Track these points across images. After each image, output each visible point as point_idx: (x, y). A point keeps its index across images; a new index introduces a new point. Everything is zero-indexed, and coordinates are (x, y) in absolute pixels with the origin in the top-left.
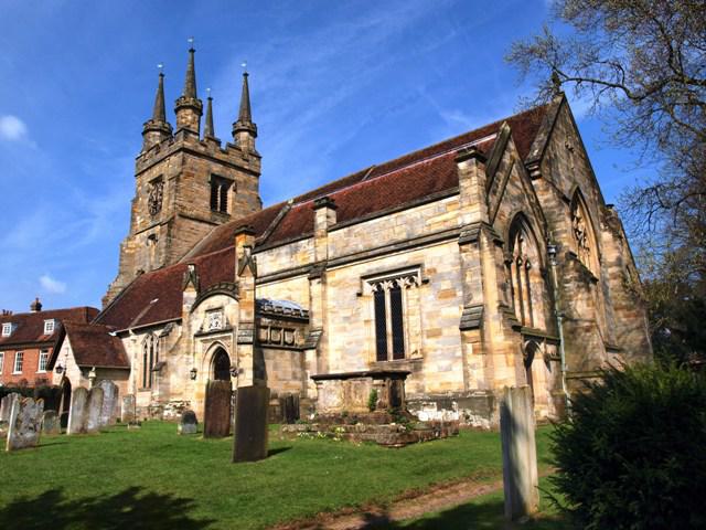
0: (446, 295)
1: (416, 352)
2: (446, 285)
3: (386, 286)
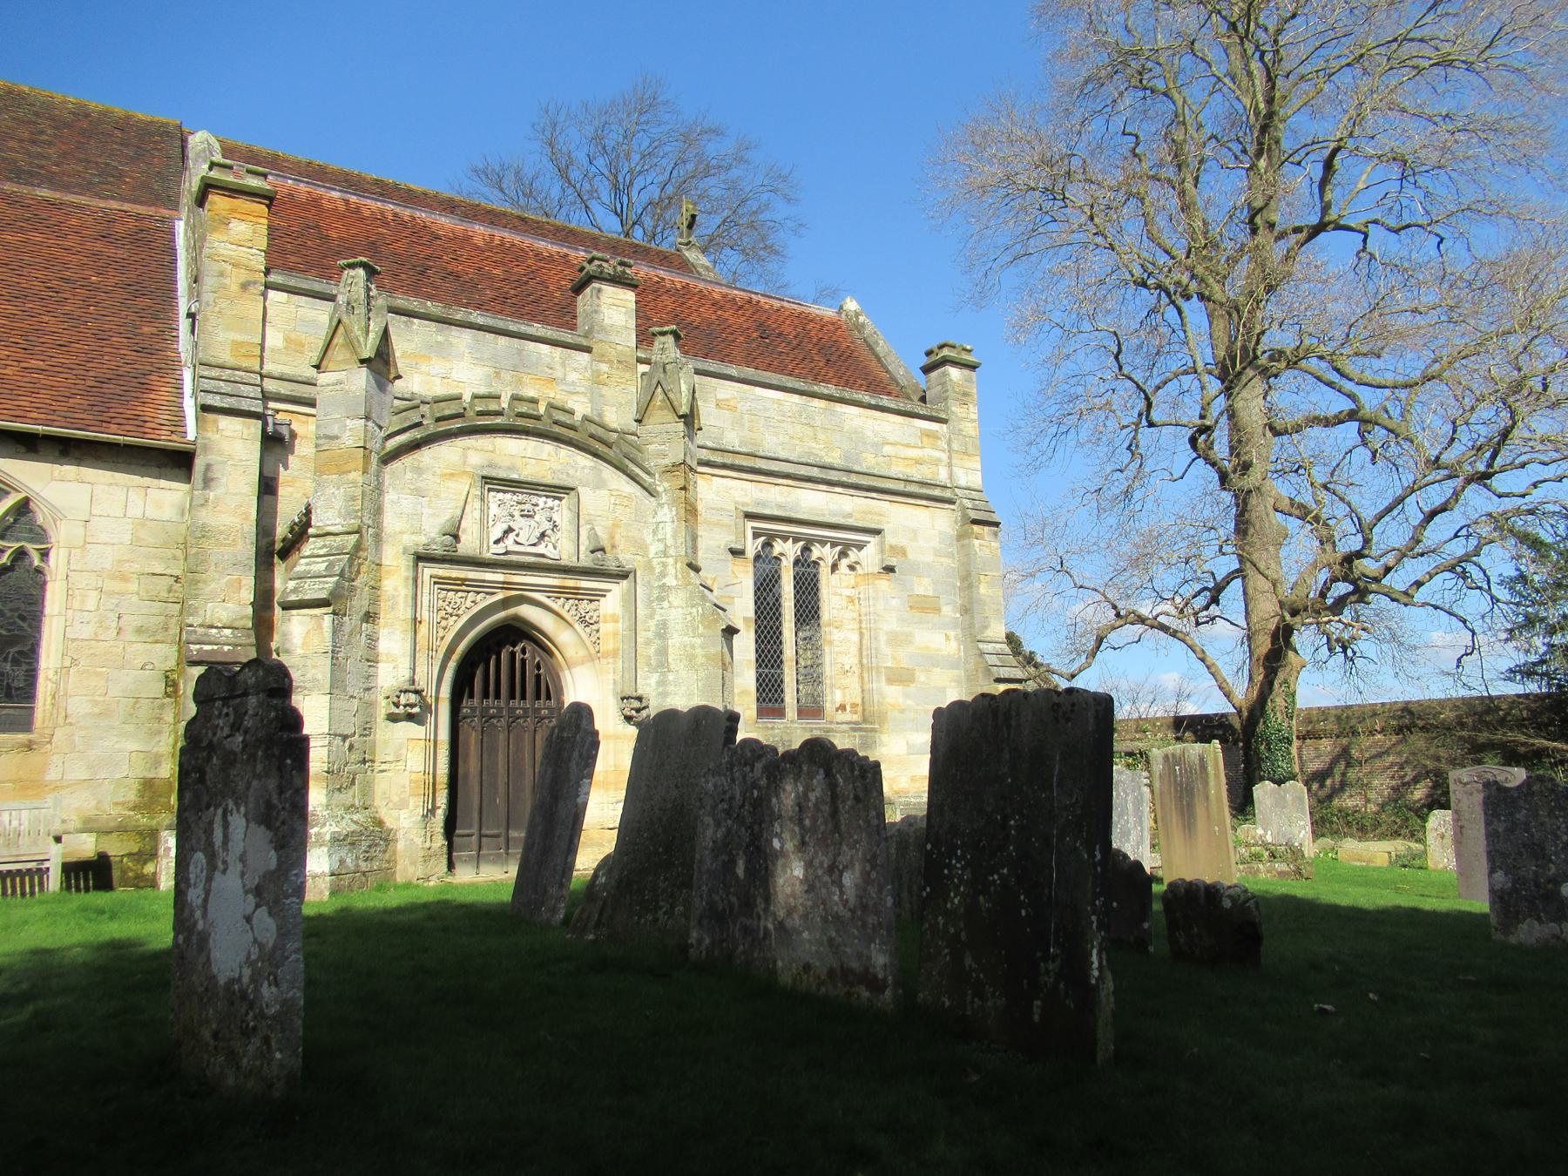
0: (924, 607)
1: (842, 708)
2: (923, 587)
3: (788, 551)
